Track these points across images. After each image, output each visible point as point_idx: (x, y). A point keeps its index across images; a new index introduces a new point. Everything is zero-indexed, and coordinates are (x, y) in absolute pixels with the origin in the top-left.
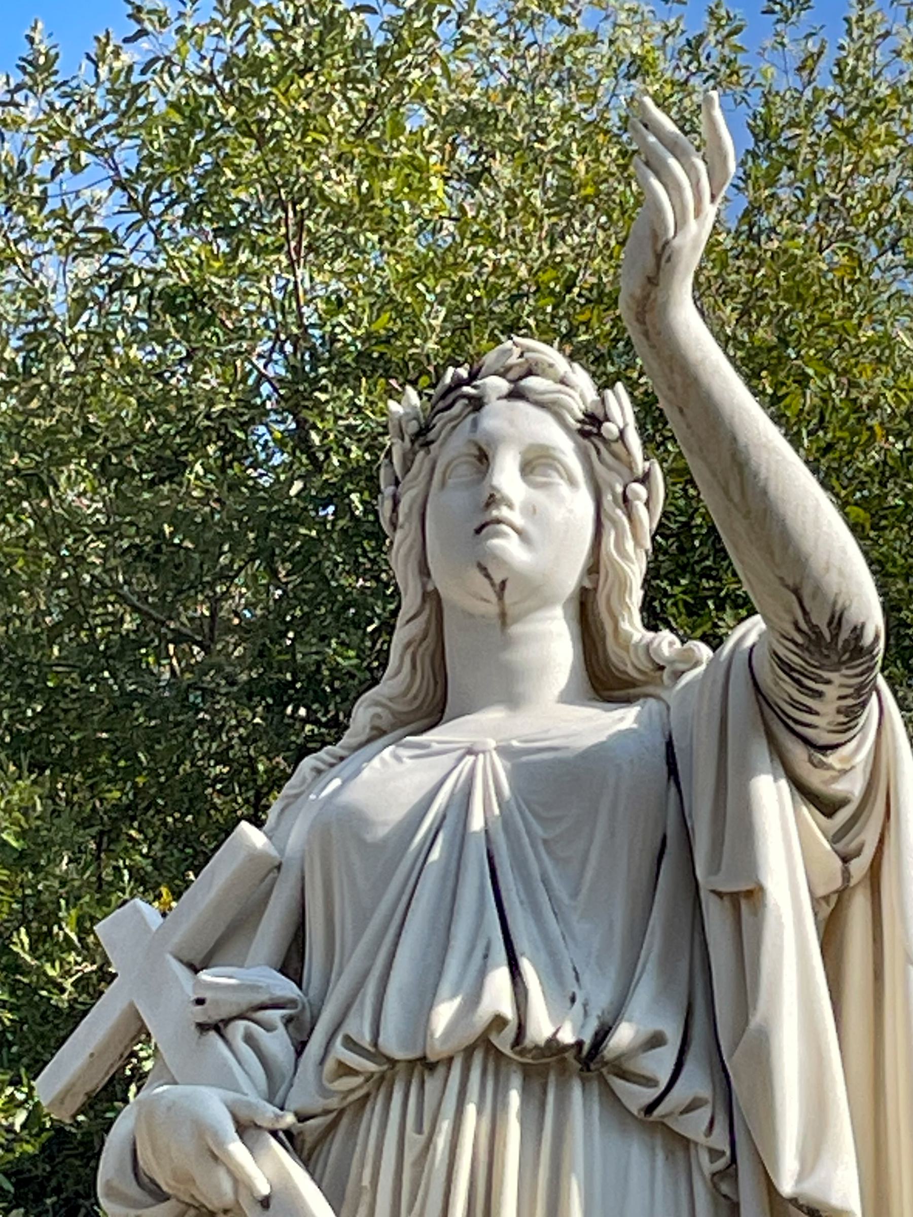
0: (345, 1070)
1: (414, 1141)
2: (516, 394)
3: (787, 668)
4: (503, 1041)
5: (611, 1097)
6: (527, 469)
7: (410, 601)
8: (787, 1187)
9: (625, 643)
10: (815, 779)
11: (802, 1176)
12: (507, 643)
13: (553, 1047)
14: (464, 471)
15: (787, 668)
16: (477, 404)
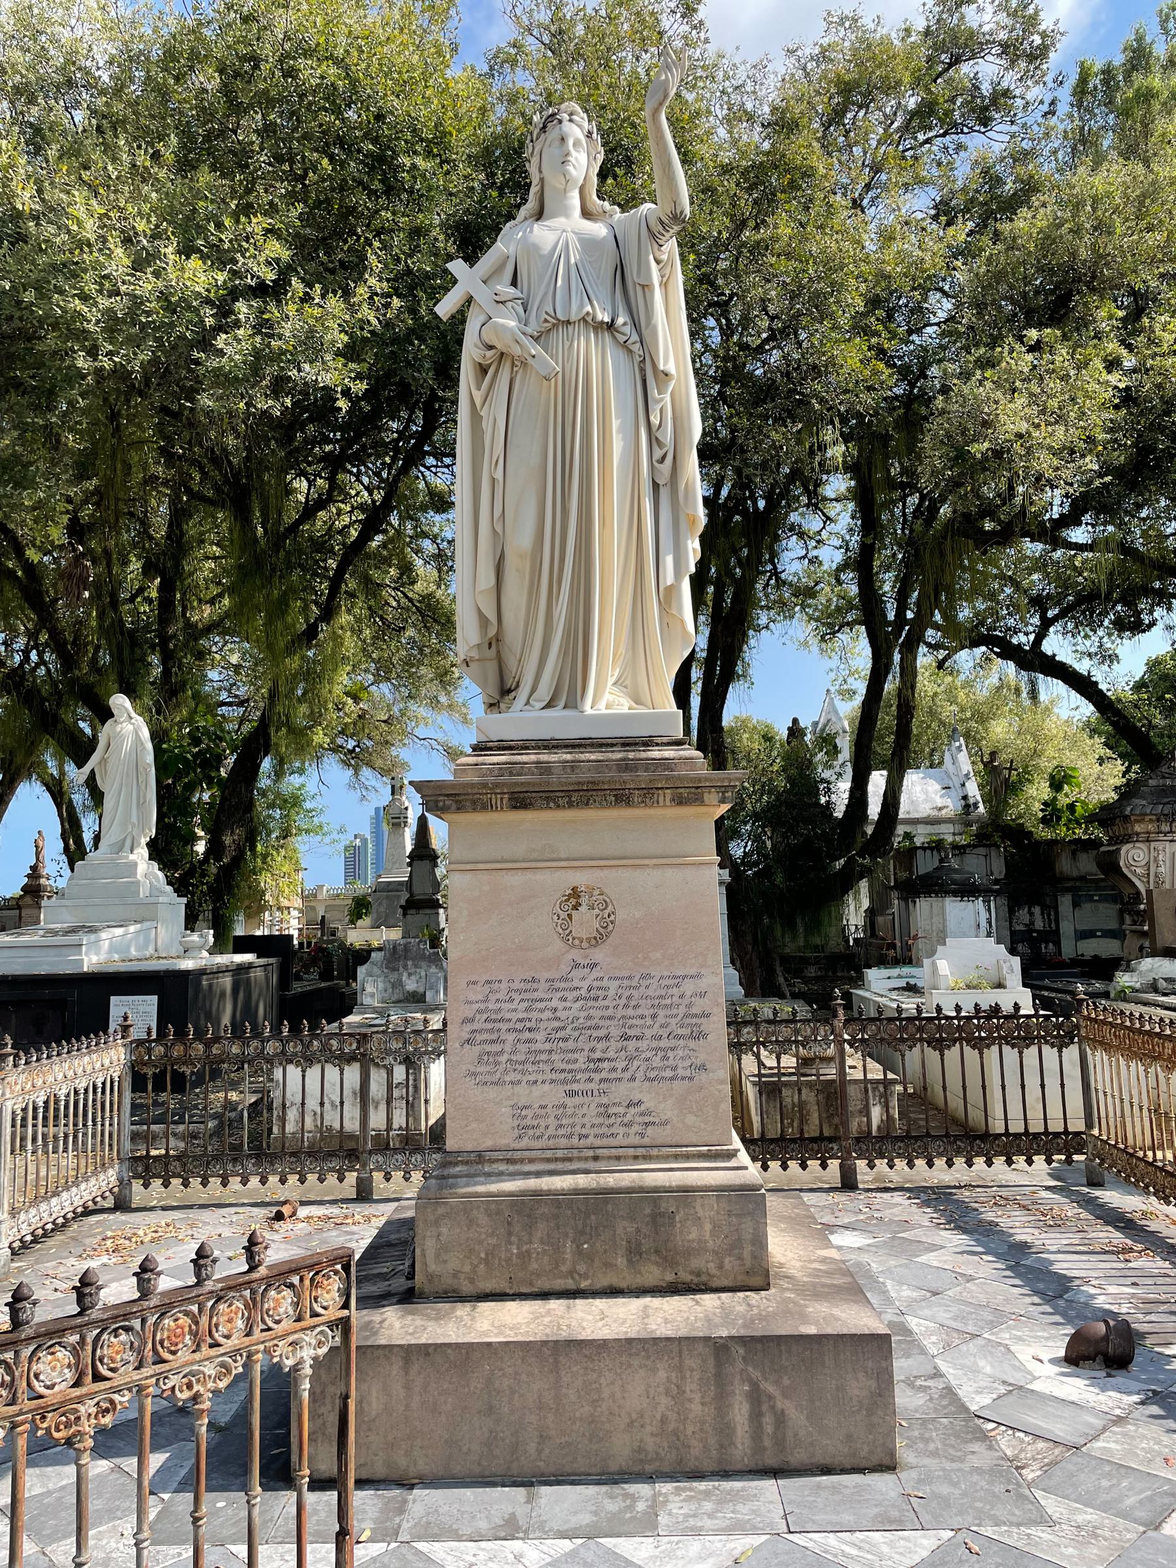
0: (546, 321)
1: (567, 344)
2: (571, 120)
3: (662, 222)
4: (589, 319)
5: (614, 337)
6: (574, 145)
7: (535, 180)
8: (661, 367)
9: (594, 204)
10: (657, 254)
11: (665, 364)
12: (565, 198)
13: (602, 322)
14: (557, 143)
15: (662, 222)
16: (560, 122)
